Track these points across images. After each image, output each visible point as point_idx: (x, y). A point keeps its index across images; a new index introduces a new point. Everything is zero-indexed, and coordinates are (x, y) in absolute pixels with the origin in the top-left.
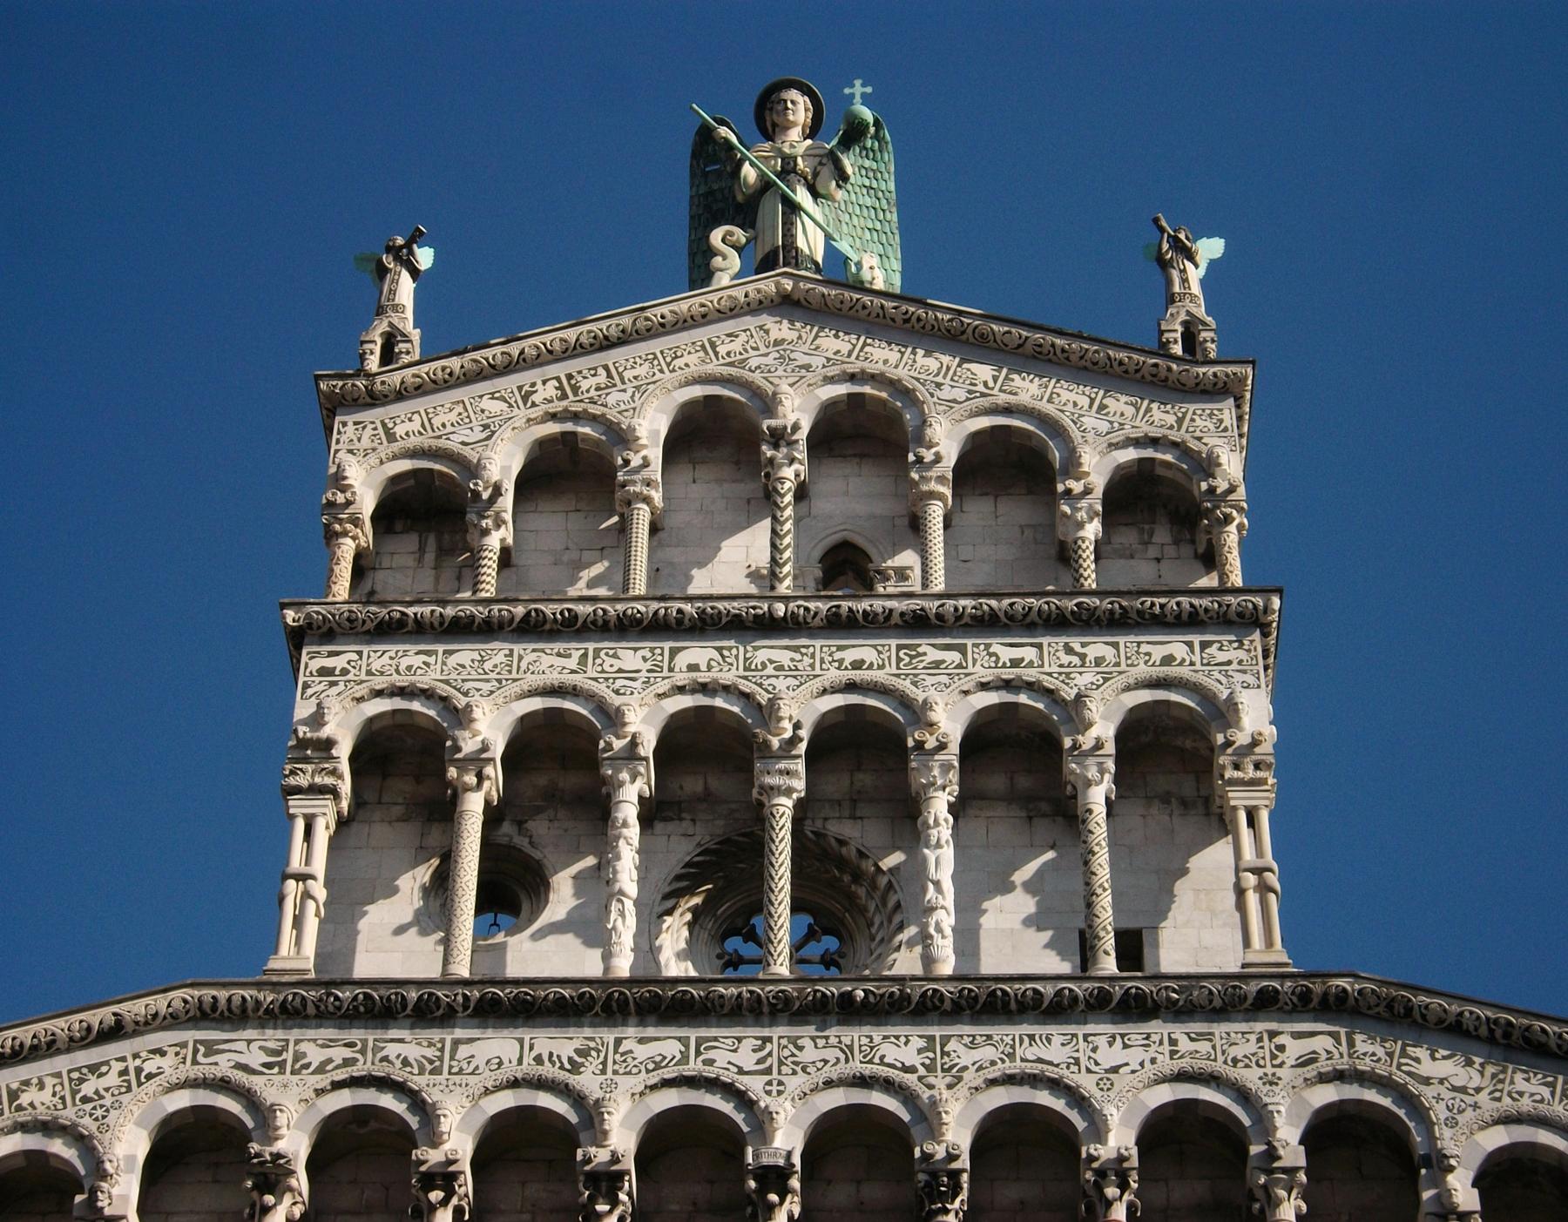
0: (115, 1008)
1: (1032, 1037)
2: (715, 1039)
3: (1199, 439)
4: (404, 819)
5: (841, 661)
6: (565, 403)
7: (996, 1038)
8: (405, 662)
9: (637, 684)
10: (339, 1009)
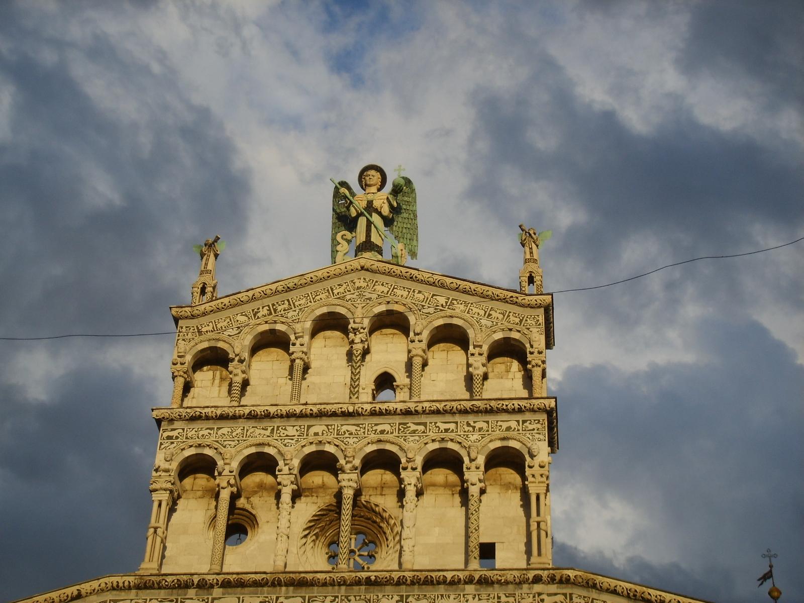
0: (78, 587)
1: (442, 596)
2: (316, 597)
3: (528, 329)
4: (202, 497)
5: (376, 431)
6: (271, 316)
7: (428, 596)
8: (201, 433)
9: (293, 442)
10: (167, 585)
